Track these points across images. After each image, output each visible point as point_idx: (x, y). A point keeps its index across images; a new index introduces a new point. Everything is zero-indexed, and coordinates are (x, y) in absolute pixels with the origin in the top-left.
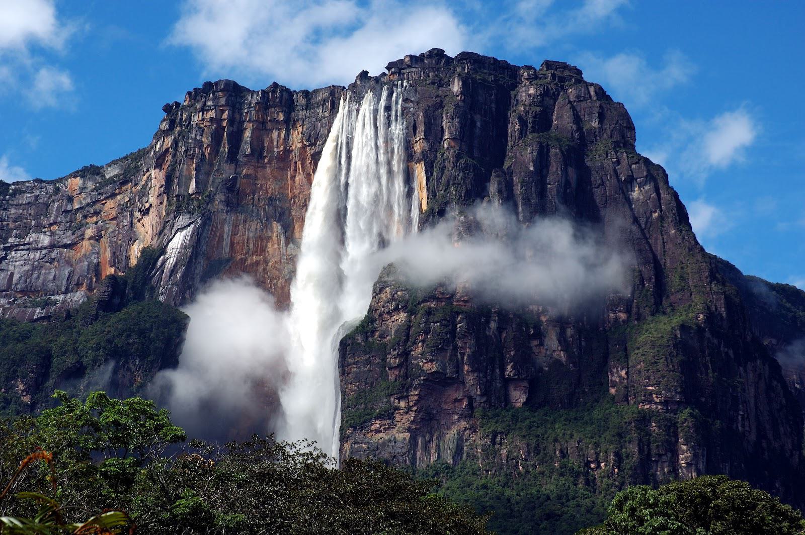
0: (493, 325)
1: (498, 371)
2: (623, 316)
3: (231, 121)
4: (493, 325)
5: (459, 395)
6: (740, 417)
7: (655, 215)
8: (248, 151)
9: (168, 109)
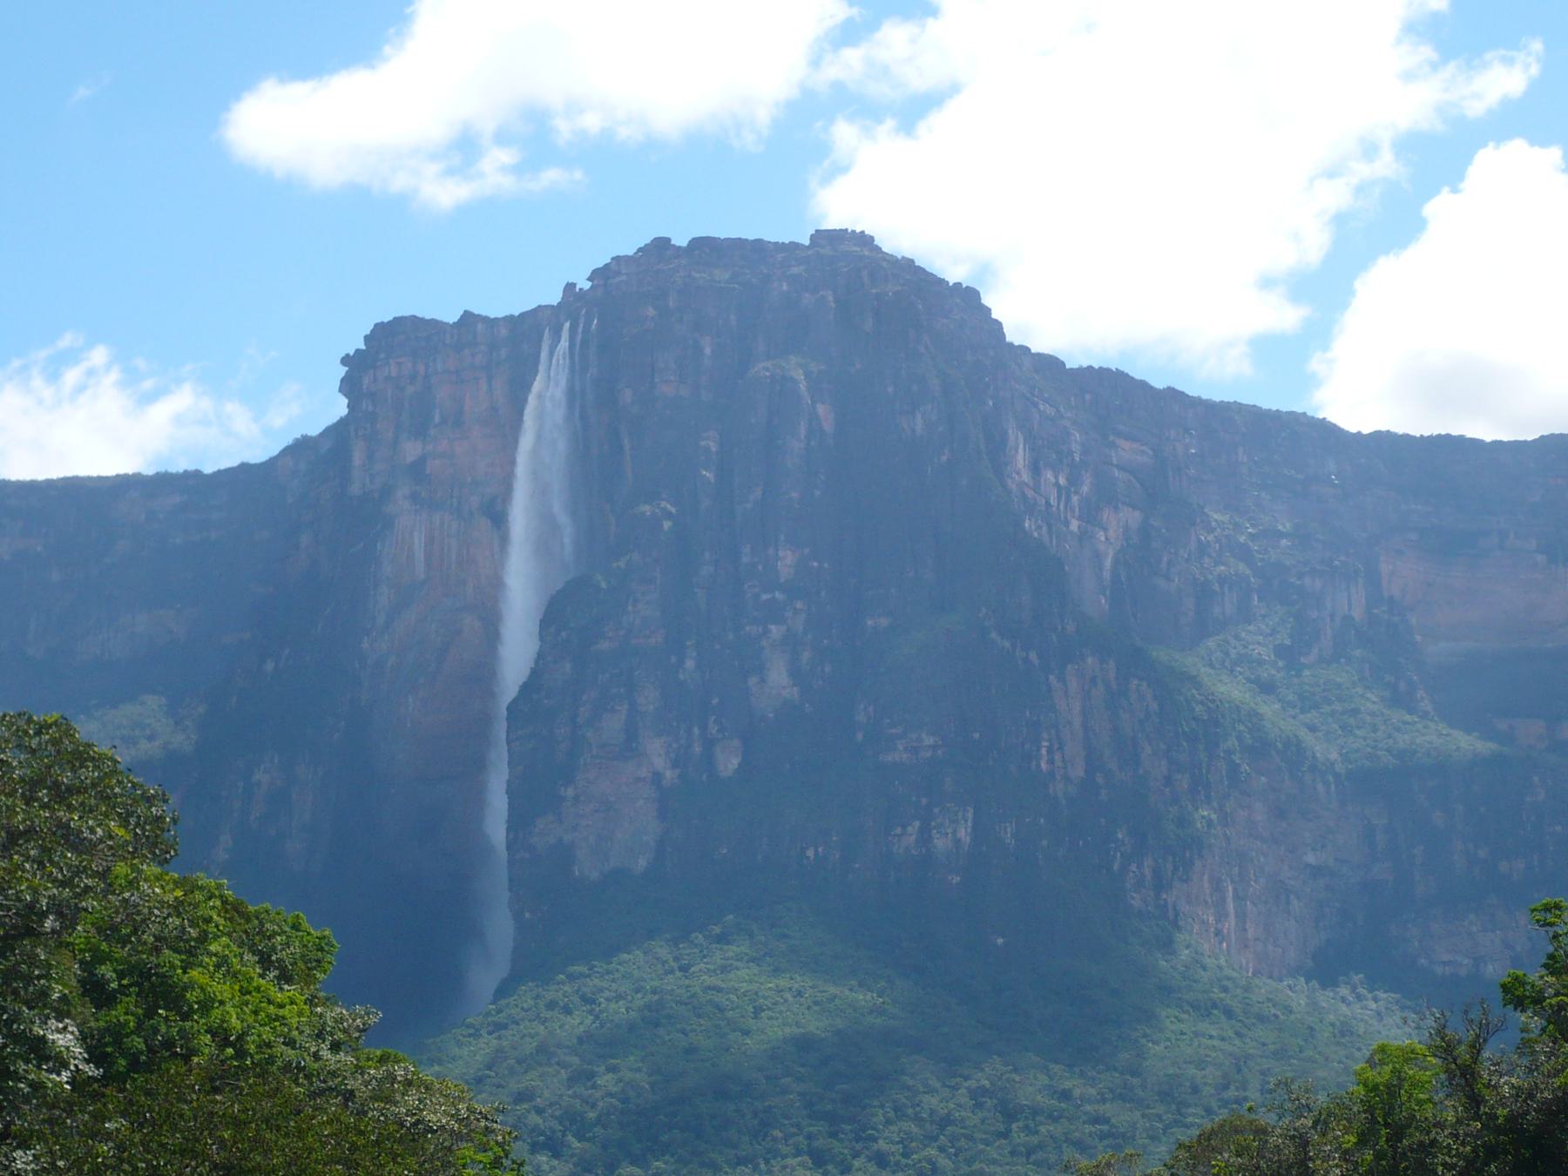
0: (690, 664)
1: (696, 730)
2: (884, 622)
4: (690, 664)
6: (1044, 751)
7: (944, 458)
8: (437, 419)
9: (346, 360)
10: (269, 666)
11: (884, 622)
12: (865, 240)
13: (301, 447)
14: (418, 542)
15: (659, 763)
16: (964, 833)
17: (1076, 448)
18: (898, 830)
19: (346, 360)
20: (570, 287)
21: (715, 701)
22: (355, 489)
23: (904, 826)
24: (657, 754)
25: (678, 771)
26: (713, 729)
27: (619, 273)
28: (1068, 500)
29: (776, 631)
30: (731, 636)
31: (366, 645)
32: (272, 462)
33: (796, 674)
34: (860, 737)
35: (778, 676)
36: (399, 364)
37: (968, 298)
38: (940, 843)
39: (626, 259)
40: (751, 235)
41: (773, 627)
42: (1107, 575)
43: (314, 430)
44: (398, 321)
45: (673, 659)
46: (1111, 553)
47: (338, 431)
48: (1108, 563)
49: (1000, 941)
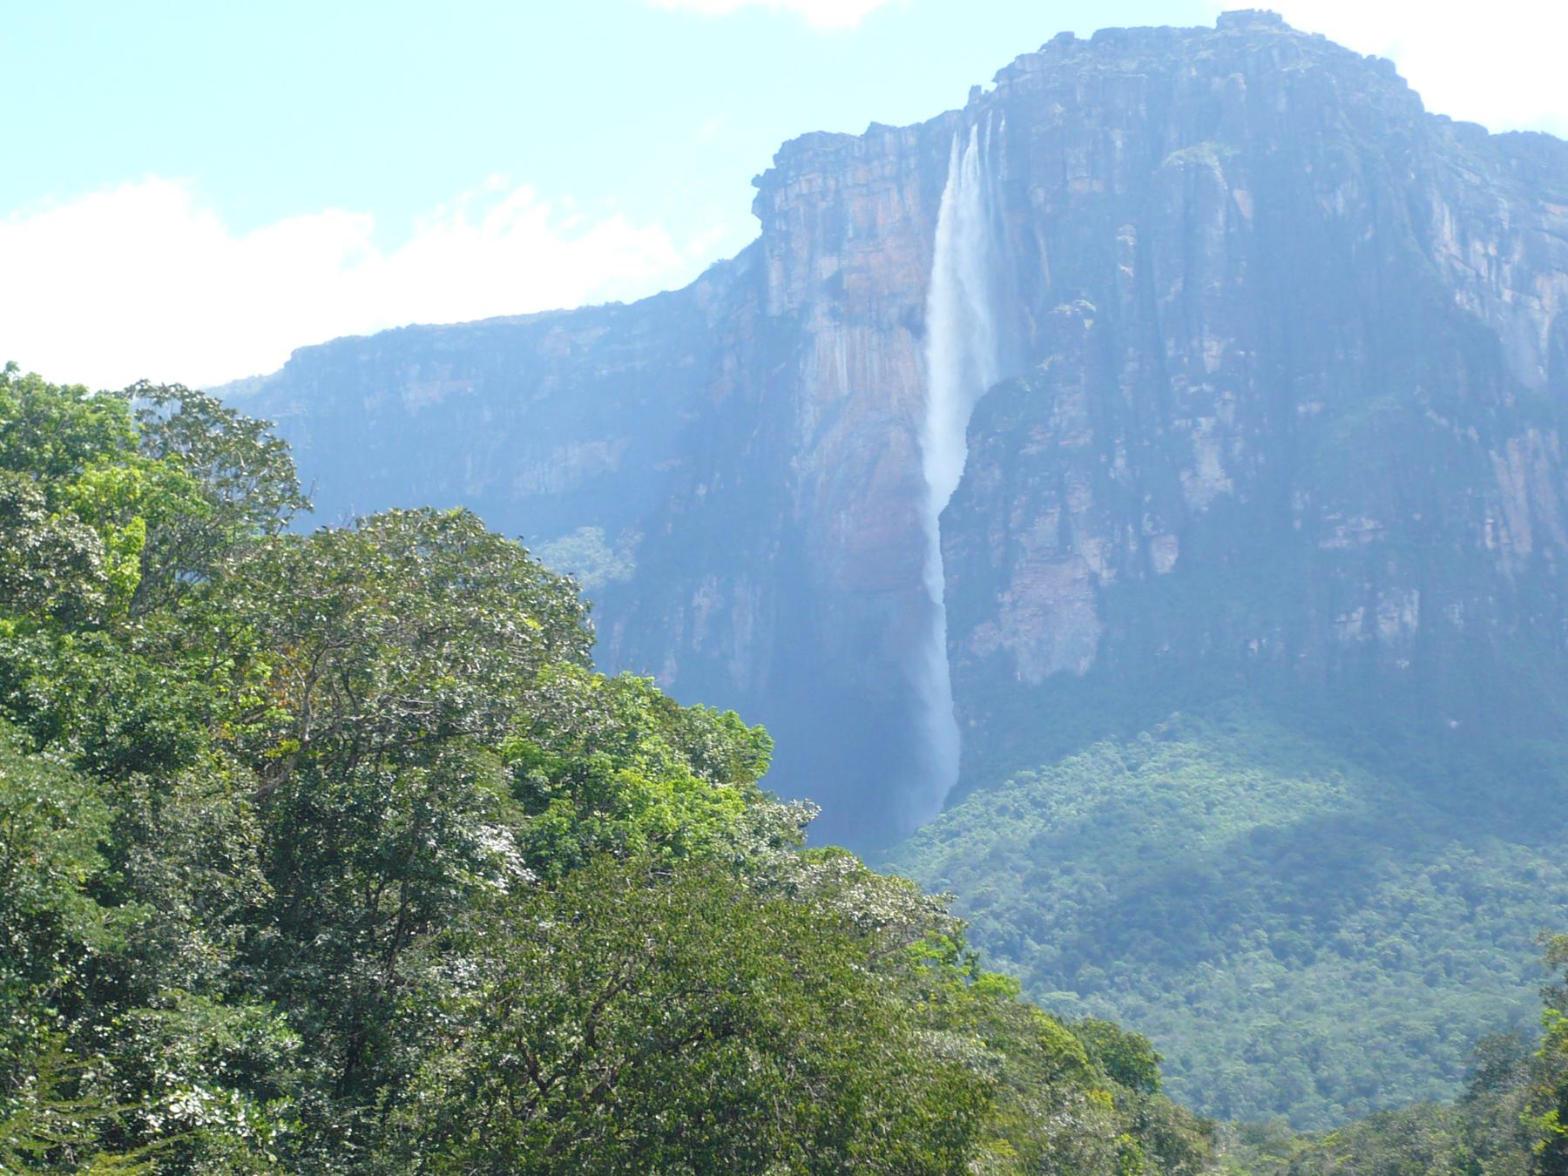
0: (1120, 462)
1: (1130, 529)
3: (824, 194)
4: (1120, 462)
5: (1079, 575)
6: (1488, 528)
7: (1368, 236)
8: (851, 234)
9: (756, 181)
10: (702, 491)
11: (1316, 407)
12: (1272, 18)
13: (717, 272)
14: (840, 358)
15: (1095, 564)
16: (1410, 617)
17: (1504, 215)
18: (1343, 618)
19: (756, 181)
20: (975, 90)
21: (1148, 498)
22: (774, 309)
23: (1348, 614)
24: (1092, 553)
25: (1114, 571)
26: (1148, 527)
27: (1023, 72)
28: (1499, 268)
29: (1205, 423)
30: (1160, 431)
31: (794, 463)
32: (691, 288)
33: (1228, 466)
34: (1298, 524)
35: (1211, 469)
36: (809, 181)
37: (1384, 68)
38: (1386, 628)
39: (1031, 57)
40: (1155, 23)
41: (1202, 420)
42: (1544, 345)
43: (730, 253)
44: (806, 138)
45: (1103, 459)
46: (1547, 321)
47: (754, 252)
48: (1544, 332)
49: (1454, 724)
